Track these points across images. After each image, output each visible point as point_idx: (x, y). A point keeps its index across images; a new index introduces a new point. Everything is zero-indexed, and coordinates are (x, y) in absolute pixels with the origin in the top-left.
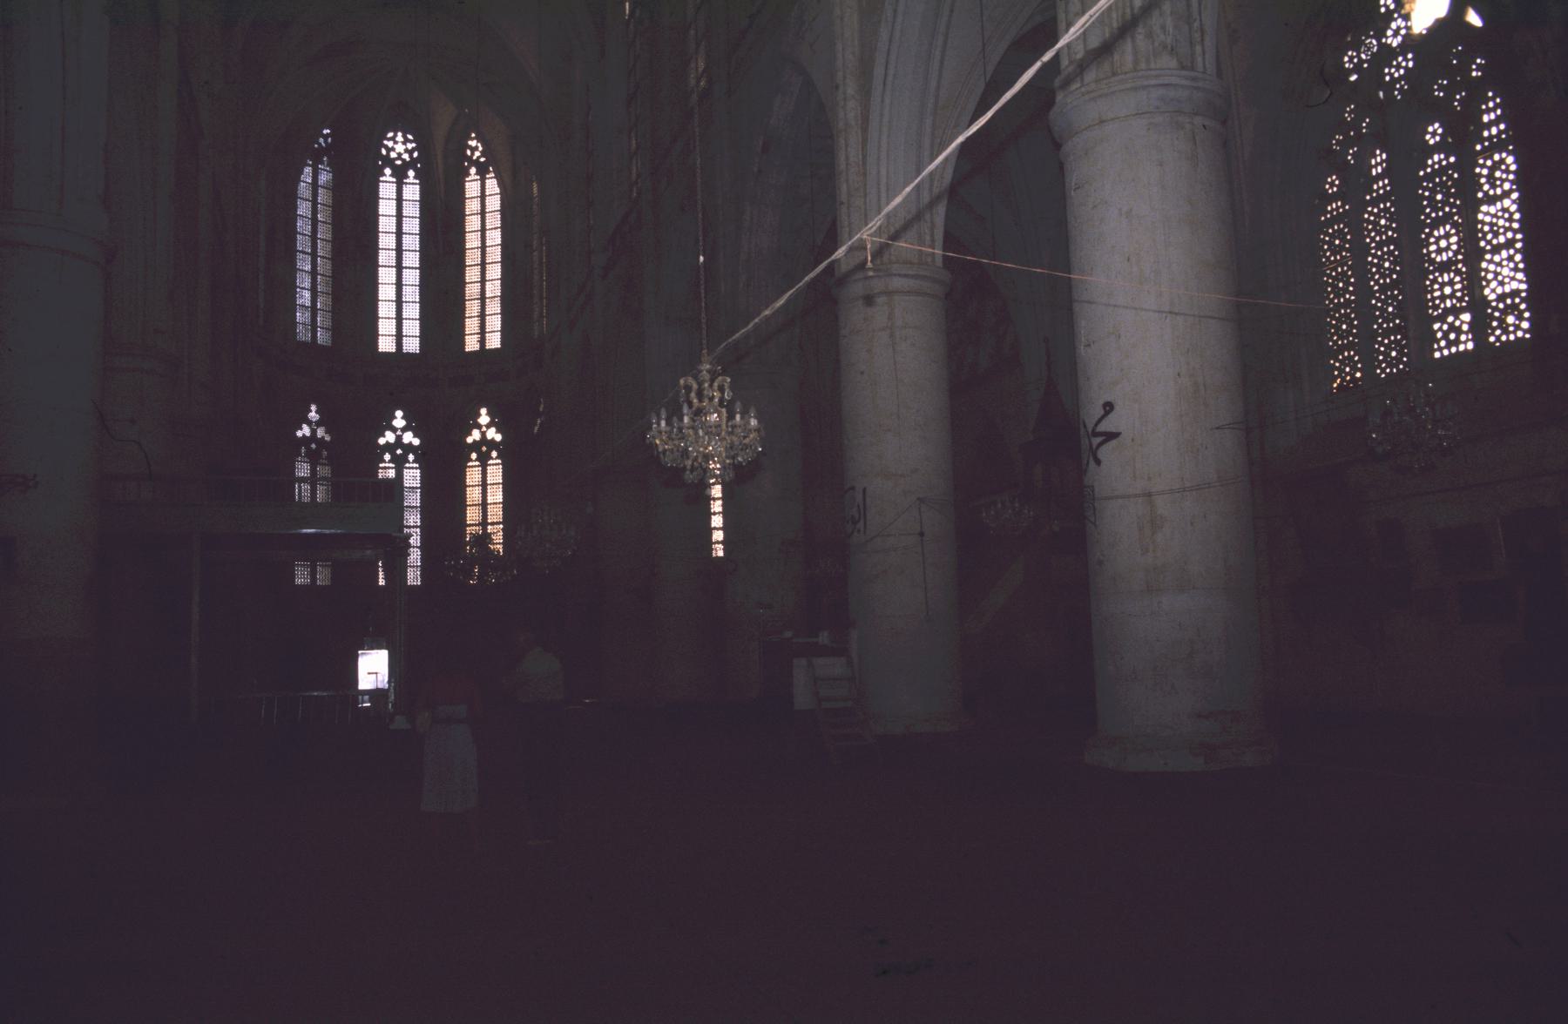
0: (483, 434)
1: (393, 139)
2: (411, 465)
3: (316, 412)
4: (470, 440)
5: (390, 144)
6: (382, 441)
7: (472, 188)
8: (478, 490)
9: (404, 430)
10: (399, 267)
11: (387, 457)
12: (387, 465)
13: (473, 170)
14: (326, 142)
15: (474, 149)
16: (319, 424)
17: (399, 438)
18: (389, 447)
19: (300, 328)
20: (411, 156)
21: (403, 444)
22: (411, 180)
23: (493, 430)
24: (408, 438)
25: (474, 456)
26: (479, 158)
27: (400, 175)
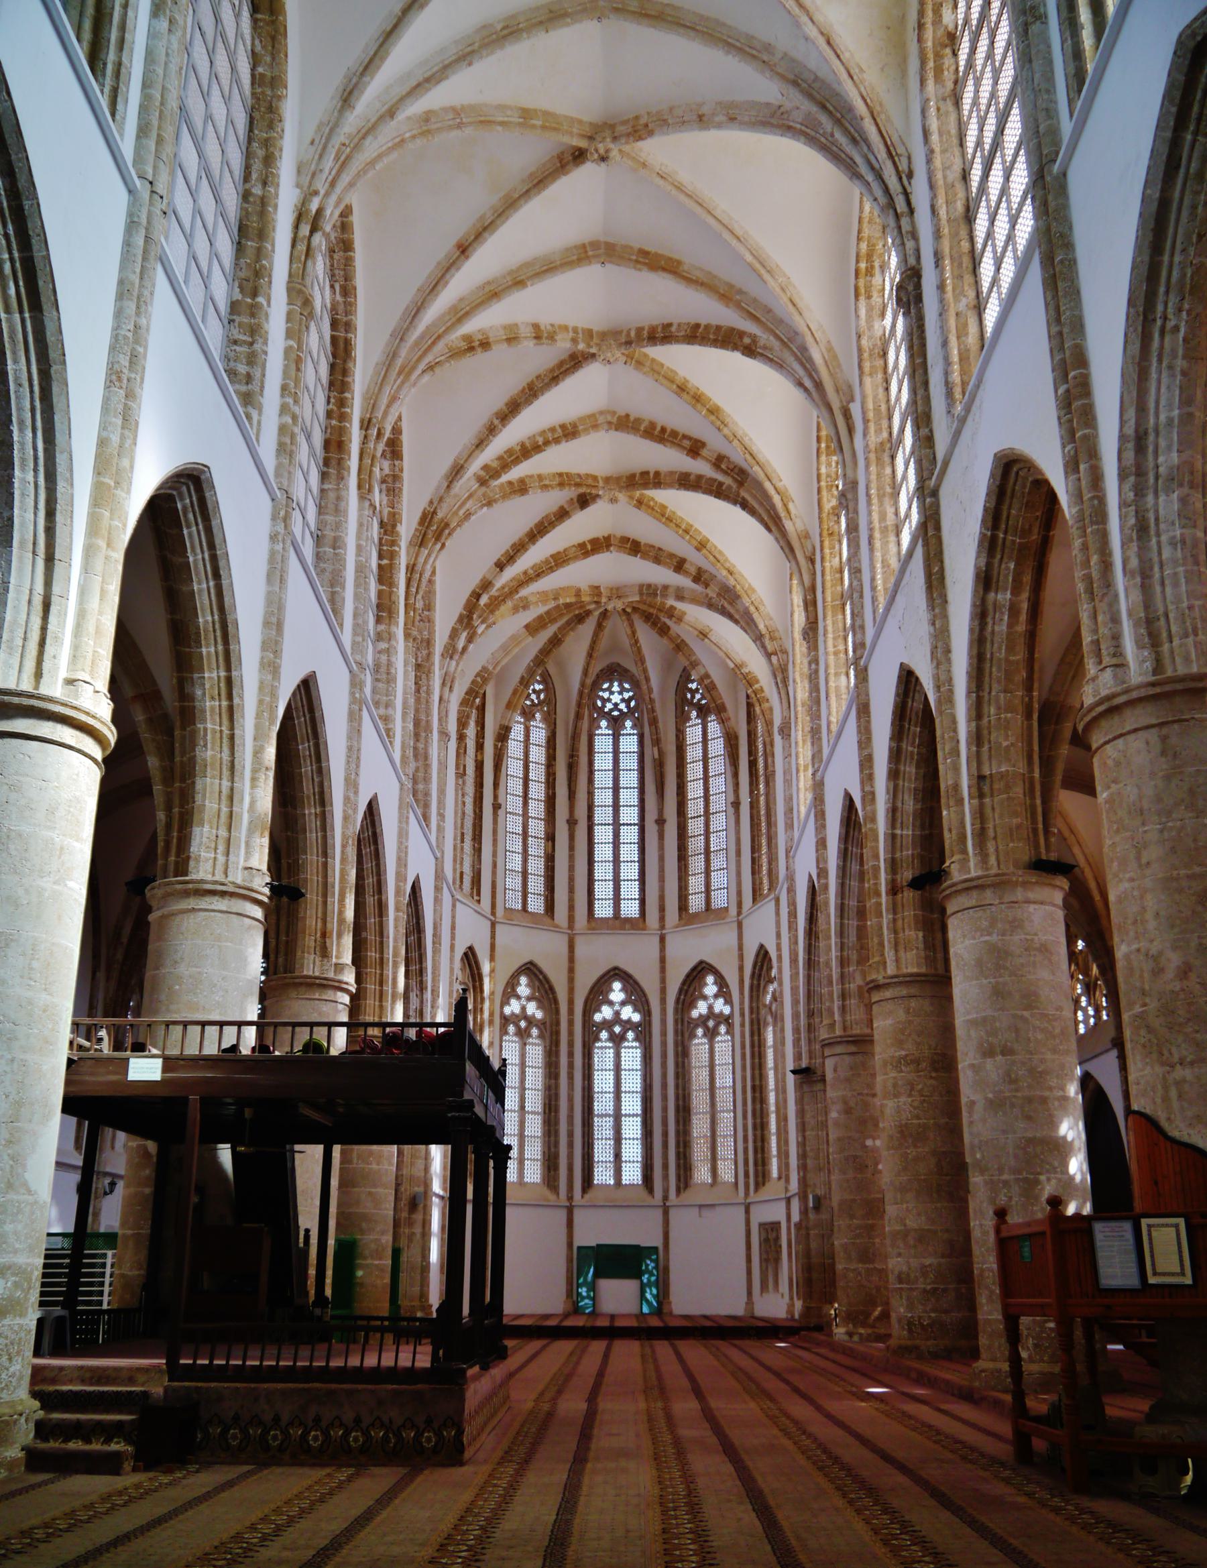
0: (710, 1007)
1: (609, 689)
2: (630, 1044)
3: (528, 985)
5: (606, 695)
6: (598, 1017)
7: (693, 733)
8: (705, 1073)
9: (623, 1003)
10: (617, 825)
11: (604, 1035)
12: (604, 1044)
13: (694, 713)
14: (538, 698)
18: (607, 1025)
19: (509, 894)
20: (628, 706)
21: (621, 1020)
23: (721, 1001)
24: (628, 1013)
25: (700, 1032)
26: (699, 700)
27: (616, 724)
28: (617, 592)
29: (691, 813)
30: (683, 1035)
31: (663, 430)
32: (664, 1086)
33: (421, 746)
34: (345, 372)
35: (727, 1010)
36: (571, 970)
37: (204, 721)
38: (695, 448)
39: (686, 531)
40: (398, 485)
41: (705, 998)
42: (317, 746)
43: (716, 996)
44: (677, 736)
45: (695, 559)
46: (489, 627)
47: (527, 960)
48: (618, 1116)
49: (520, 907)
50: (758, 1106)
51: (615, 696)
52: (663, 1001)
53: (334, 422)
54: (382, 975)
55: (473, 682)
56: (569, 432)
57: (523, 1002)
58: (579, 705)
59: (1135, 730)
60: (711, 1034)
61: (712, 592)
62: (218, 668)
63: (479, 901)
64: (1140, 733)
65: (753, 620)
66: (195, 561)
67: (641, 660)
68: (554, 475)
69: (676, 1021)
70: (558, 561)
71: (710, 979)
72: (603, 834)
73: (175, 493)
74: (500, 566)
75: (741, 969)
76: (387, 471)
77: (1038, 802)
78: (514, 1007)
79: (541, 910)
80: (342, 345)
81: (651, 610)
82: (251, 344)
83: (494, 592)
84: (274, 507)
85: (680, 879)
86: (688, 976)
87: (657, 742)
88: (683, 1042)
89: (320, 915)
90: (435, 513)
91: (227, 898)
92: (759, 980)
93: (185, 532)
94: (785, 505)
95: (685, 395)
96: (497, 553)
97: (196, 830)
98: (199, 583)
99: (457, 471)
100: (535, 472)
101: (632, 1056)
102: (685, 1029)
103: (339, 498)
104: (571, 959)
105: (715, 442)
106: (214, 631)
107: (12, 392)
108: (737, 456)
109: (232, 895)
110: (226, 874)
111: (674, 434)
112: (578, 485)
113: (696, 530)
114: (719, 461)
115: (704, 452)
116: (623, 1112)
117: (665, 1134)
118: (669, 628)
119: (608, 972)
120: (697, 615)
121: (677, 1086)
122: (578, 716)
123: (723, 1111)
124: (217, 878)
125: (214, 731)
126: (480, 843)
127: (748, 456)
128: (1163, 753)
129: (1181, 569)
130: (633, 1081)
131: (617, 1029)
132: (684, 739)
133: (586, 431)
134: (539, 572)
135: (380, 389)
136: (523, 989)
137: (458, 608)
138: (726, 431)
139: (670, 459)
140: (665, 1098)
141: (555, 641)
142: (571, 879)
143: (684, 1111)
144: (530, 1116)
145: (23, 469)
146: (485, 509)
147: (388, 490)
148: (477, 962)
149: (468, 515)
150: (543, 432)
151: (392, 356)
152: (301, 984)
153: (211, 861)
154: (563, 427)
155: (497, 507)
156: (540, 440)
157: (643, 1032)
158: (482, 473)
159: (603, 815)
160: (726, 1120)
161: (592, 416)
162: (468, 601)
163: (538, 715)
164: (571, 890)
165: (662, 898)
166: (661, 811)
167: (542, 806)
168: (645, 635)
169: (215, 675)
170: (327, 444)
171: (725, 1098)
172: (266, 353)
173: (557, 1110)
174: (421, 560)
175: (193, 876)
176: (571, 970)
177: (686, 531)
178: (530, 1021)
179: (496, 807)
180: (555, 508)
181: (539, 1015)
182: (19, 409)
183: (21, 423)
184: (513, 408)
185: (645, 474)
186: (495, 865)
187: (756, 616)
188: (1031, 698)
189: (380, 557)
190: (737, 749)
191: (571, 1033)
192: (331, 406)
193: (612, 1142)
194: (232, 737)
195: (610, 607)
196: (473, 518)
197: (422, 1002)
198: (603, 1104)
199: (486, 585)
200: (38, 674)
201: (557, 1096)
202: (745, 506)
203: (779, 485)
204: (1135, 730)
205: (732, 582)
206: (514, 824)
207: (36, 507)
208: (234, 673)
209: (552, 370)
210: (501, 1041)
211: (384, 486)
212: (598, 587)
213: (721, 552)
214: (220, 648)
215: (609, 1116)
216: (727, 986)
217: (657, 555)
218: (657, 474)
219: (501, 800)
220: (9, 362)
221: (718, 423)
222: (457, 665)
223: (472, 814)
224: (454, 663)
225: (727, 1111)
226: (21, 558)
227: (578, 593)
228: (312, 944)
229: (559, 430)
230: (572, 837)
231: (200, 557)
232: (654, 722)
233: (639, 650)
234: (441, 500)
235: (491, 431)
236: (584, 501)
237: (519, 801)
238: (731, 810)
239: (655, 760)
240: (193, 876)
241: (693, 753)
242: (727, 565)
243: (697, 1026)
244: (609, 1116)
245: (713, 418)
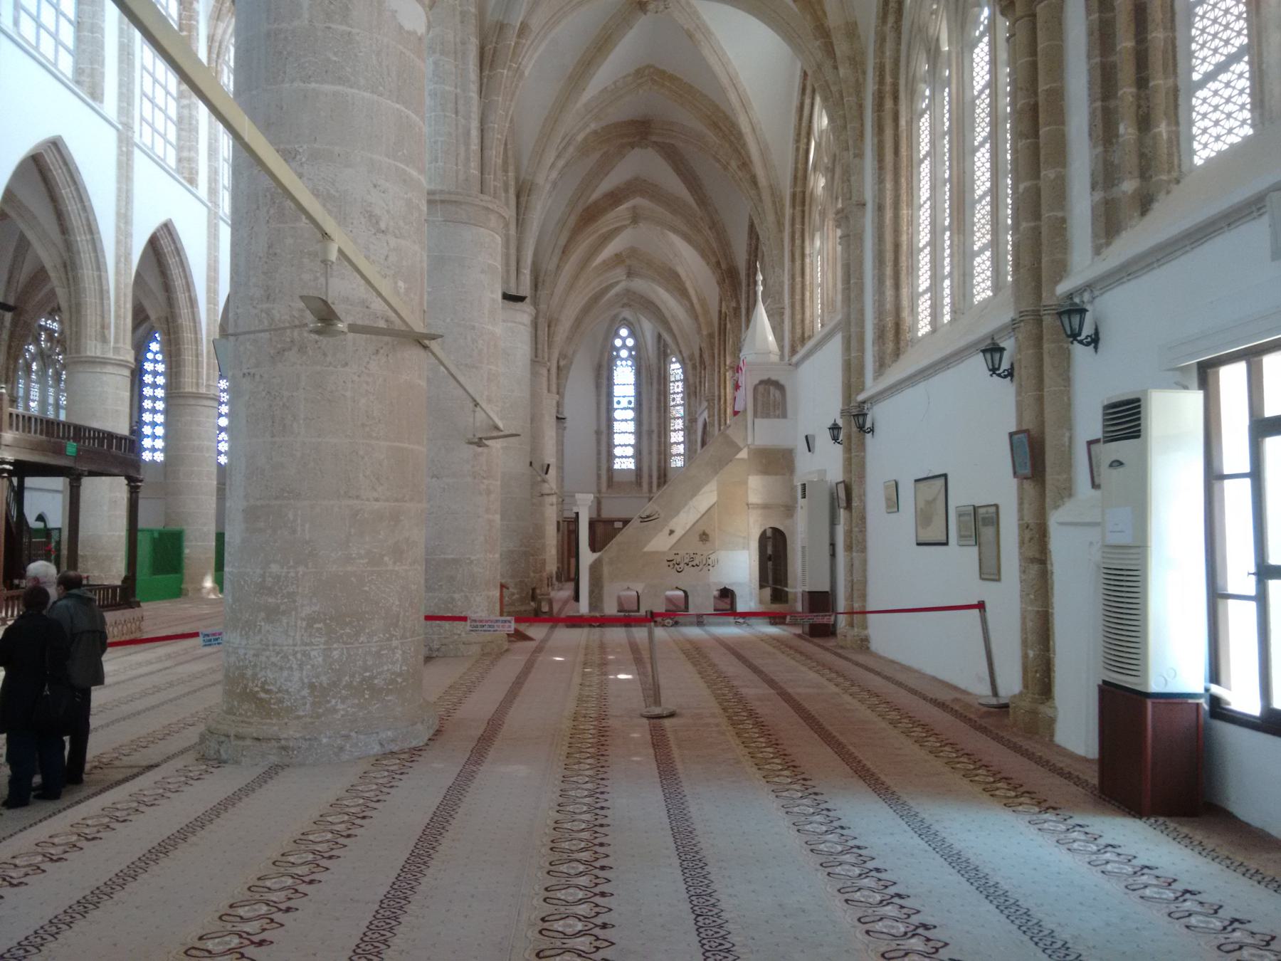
54: (197, 350)
77: (513, 251)
89: (99, 313)
129: (433, 113)
152: (86, 362)
174: (220, 31)
188: (507, 177)
228: (93, 334)
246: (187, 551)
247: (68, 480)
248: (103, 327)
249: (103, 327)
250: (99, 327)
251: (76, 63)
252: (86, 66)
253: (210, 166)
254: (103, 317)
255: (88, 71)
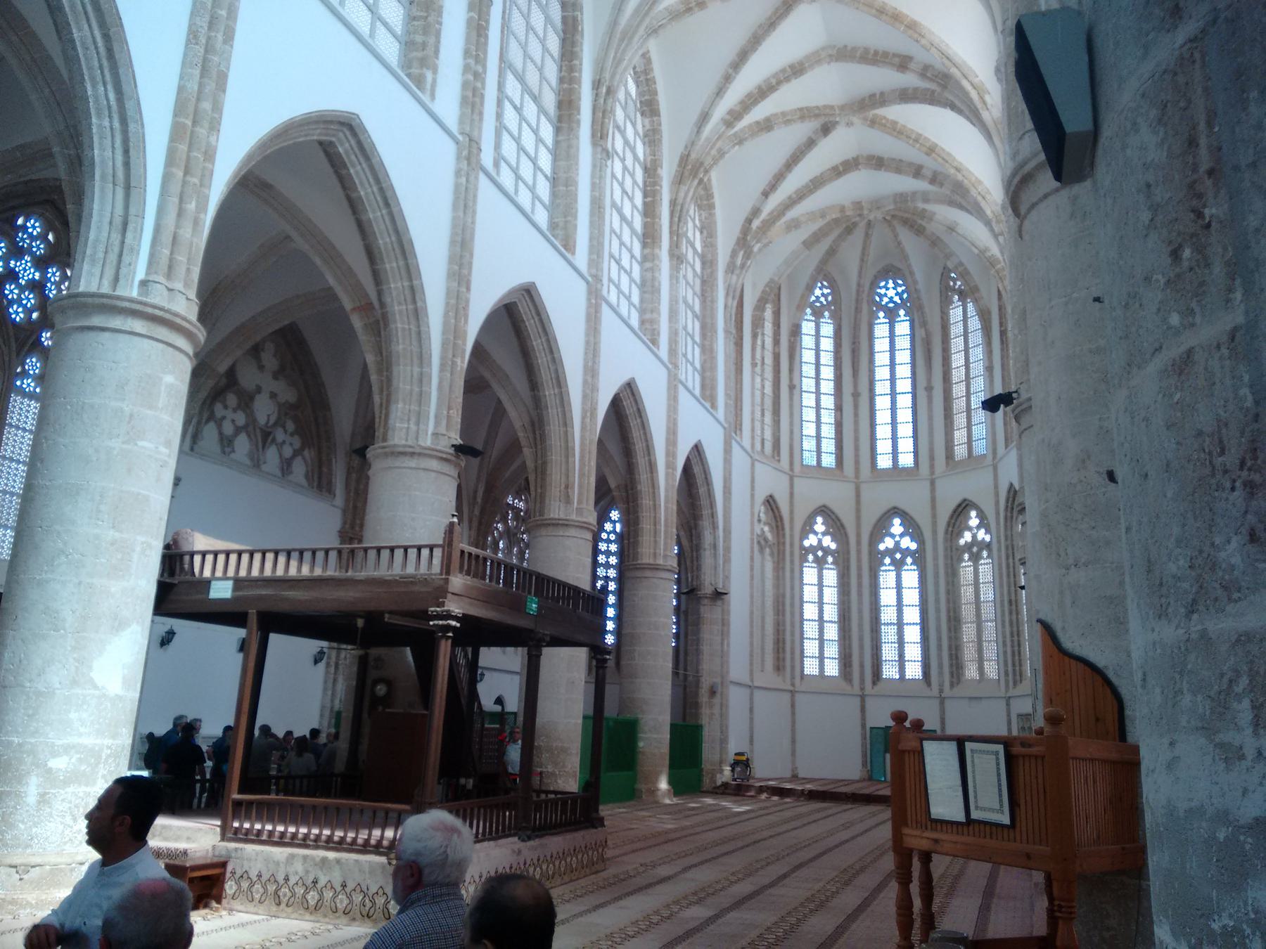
0: (974, 536)
2: (909, 567)
4: (962, 542)
5: (883, 291)
6: (882, 547)
7: (956, 313)
8: (971, 589)
9: (902, 535)
10: (893, 394)
11: (887, 560)
12: (887, 568)
15: (954, 280)
16: (824, 534)
17: (897, 543)
18: (889, 552)
19: (806, 454)
22: (903, 318)
25: (966, 556)
27: (892, 315)
28: (876, 204)
29: (955, 380)
30: (952, 559)
31: (876, 53)
32: (937, 601)
33: (707, 343)
34: (573, 44)
35: (988, 538)
36: (858, 510)
37: (395, 322)
38: (903, 63)
39: (916, 141)
40: (657, 137)
41: (970, 529)
42: (548, 341)
43: (978, 527)
44: (942, 318)
45: (929, 164)
46: (766, 245)
47: (821, 504)
48: (900, 625)
49: (815, 463)
50: (1014, 617)
51: (890, 292)
52: (935, 532)
53: (565, 86)
55: (763, 292)
56: (796, 70)
57: (820, 536)
58: (858, 301)
59: (1046, 196)
60: (975, 558)
61: (946, 191)
62: (401, 279)
63: (779, 461)
64: (1051, 199)
65: (981, 209)
66: (366, 193)
67: (905, 257)
68: (795, 110)
69: (946, 549)
70: (816, 184)
71: (973, 514)
72: (882, 403)
73: (333, 139)
74: (766, 194)
75: (997, 503)
76: (648, 127)
78: (811, 541)
79: (833, 465)
80: (570, 21)
81: (906, 215)
82: (427, 17)
83: (764, 215)
84: (458, 149)
85: (946, 434)
86: (955, 511)
87: (924, 324)
88: (952, 565)
90: (688, 155)
91: (416, 457)
92: (1012, 513)
93: (352, 171)
94: (982, 98)
95: (884, 17)
96: (762, 185)
97: (393, 407)
98: (374, 212)
99: (704, 117)
100: (774, 111)
101: (911, 577)
102: (953, 555)
103: (569, 147)
104: (858, 502)
105: (920, 56)
106: (394, 250)
107: (81, 56)
108: (937, 62)
109: (420, 454)
110: (417, 438)
111: (885, 54)
112: (817, 116)
113: (926, 138)
114: (926, 71)
115: (912, 66)
116: (905, 622)
117: (939, 639)
118: (924, 228)
119: (889, 511)
120: (945, 213)
121: (948, 601)
122: (858, 310)
123: (987, 621)
124: (410, 443)
125: (404, 329)
126: (779, 416)
127: (945, 60)
128: (1072, 216)
130: (912, 596)
131: (898, 556)
132: (948, 320)
133: (812, 67)
134: (800, 195)
135: (606, 54)
136: (820, 526)
137: (736, 232)
138: (923, 41)
139: (884, 78)
140: (938, 610)
141: (831, 252)
142: (857, 439)
143: (955, 621)
144: (828, 624)
145: (99, 116)
146: (737, 147)
147: (650, 142)
148: (778, 508)
149: (722, 154)
150: (775, 75)
151: (614, 23)
152: (549, 525)
153: (404, 430)
154: (792, 67)
155: (748, 144)
156: (774, 81)
157: (919, 558)
158: (728, 117)
159: (882, 387)
160: (990, 629)
161: (817, 52)
162: (743, 225)
163: (826, 314)
164: (857, 448)
165: (931, 450)
166: (929, 380)
167: (832, 384)
168: (906, 236)
169: (399, 284)
170: (560, 105)
171: (988, 611)
172: (440, 24)
173: (849, 620)
174: (682, 195)
175: (391, 443)
176: (858, 510)
177: (916, 141)
178: (827, 551)
179: (792, 387)
180: (805, 139)
181: (833, 546)
182: (90, 68)
183: (93, 79)
184: (743, 57)
185: (872, 96)
186: (792, 432)
187: (983, 204)
189: (645, 195)
190: (990, 322)
191: (859, 560)
192: (563, 73)
193: (897, 645)
194: (419, 333)
195: (871, 217)
196: (727, 156)
197: (715, 538)
198: (888, 615)
199: (756, 212)
200: (116, 279)
201: (849, 608)
202: (953, 107)
203: (976, 81)
204: (1046, 196)
205: (960, 177)
206: (808, 400)
207: (113, 147)
208: (415, 282)
209: (770, 18)
210: (802, 567)
211: (646, 139)
212: (859, 203)
213: (949, 154)
214: (401, 263)
215: (894, 624)
216: (987, 519)
217: (898, 166)
218: (882, 94)
219: (796, 382)
220: (74, 31)
221: (916, 36)
222: (738, 278)
223: (771, 394)
224: (734, 277)
225: (991, 621)
226: (102, 190)
227: (842, 209)
229: (789, 70)
230: (856, 406)
231: (369, 190)
232: (920, 308)
233: (903, 251)
234: (693, 143)
235: (727, 79)
236: (826, 130)
237: (813, 382)
238: (987, 374)
239: (923, 339)
240: (391, 443)
241: (956, 330)
242: (955, 164)
243: (964, 552)
244: (894, 624)
245: (910, 32)
246: (641, 744)
247: (526, 649)
248: (567, 487)
249: (567, 487)
250: (563, 486)
251: (551, 218)
252: (560, 220)
253: (670, 328)
254: (567, 476)
255: (561, 224)
